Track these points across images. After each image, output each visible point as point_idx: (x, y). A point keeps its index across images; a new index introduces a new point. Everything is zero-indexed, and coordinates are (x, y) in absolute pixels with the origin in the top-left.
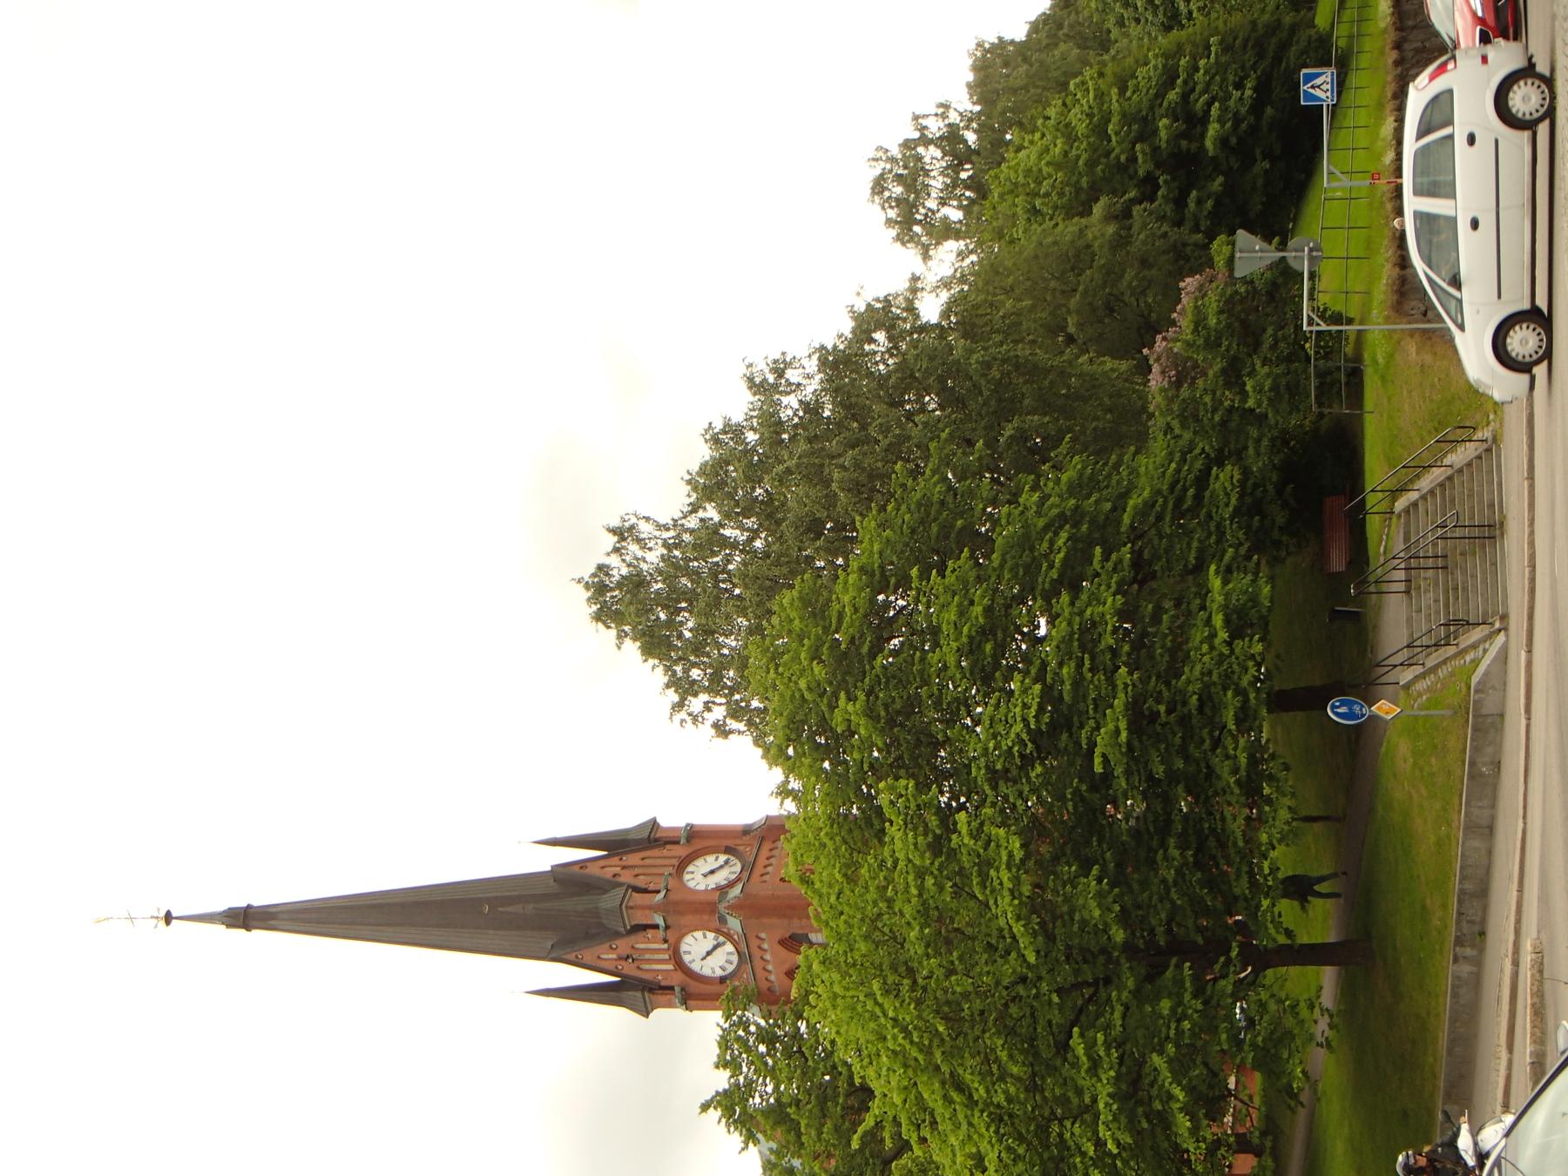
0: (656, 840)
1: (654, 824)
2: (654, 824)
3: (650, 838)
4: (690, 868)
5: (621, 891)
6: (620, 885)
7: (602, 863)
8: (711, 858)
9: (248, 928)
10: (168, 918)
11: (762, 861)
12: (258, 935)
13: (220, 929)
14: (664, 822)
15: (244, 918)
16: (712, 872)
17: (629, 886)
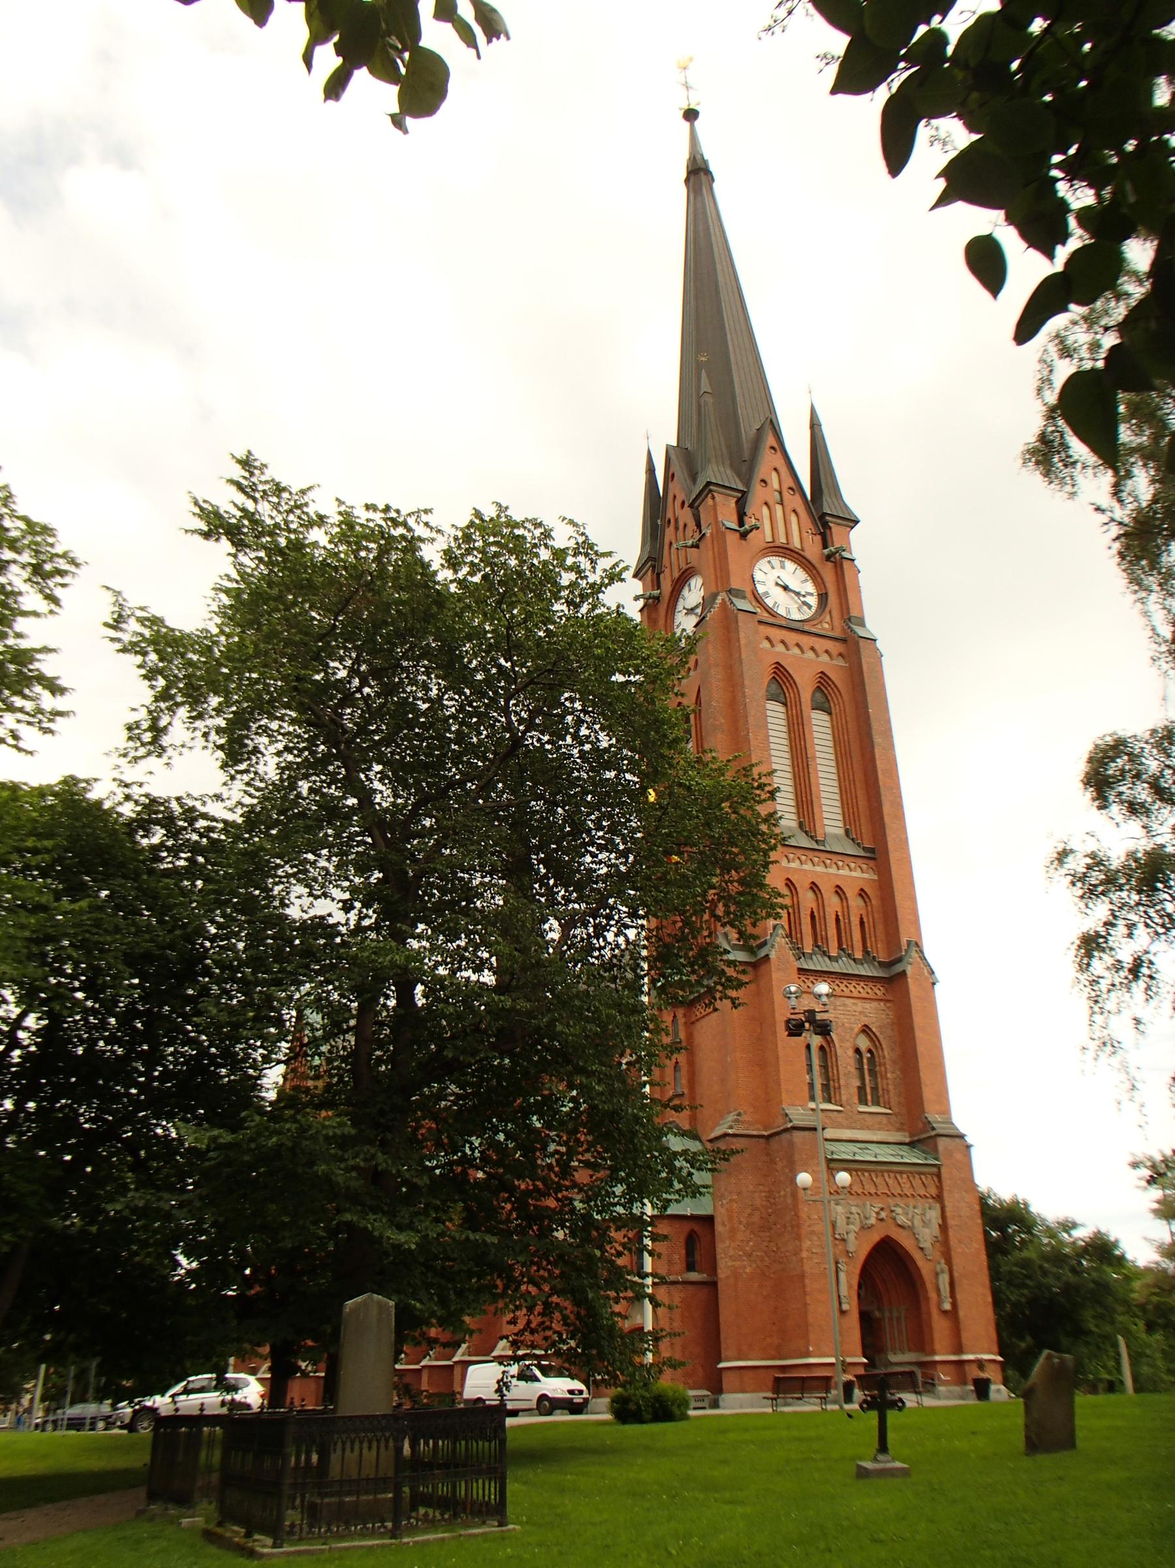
0: (825, 525)
1: (853, 522)
2: (853, 522)
3: (825, 512)
4: (790, 566)
5: (741, 487)
6: (748, 482)
7: (784, 470)
8: (810, 587)
9: (687, 181)
10: (691, 115)
11: (806, 641)
12: (679, 194)
13: (685, 156)
14: (855, 534)
15: (698, 173)
16: (785, 588)
17: (744, 493)
